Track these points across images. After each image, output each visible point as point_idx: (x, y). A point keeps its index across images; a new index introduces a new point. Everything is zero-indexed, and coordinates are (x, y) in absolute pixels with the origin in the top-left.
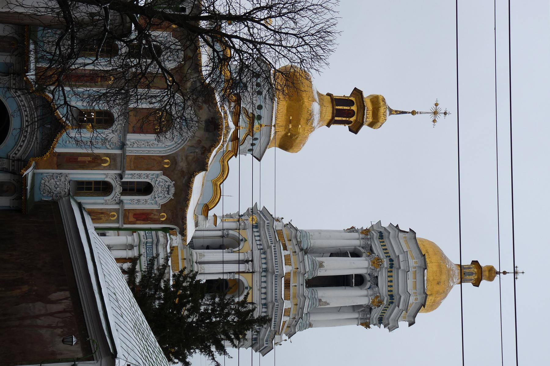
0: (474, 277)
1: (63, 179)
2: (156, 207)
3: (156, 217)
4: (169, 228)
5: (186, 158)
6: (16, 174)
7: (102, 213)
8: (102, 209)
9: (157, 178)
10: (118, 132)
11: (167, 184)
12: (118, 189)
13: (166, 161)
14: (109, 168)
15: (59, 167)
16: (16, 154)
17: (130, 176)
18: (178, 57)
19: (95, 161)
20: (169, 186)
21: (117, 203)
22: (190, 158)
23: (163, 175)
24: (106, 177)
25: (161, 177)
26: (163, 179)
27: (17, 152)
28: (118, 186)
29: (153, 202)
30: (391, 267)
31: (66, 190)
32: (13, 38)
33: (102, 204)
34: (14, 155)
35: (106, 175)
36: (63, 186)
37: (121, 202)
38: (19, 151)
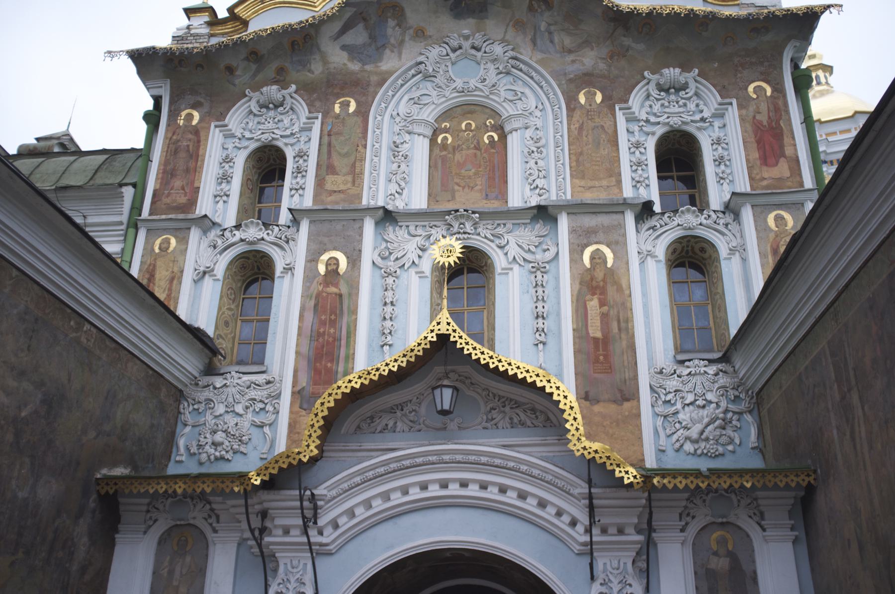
0: (821, 73)
1: (673, 384)
2: (733, 114)
3: (764, 107)
4: (792, 74)
5: (570, 51)
6: (651, 514)
7: (775, 251)
8: (763, 255)
9: (639, 121)
10: (500, 230)
11: (654, 93)
12: (689, 220)
13: (582, 99)
14: (619, 245)
15: (627, 394)
16: (573, 523)
17: (642, 191)
18: (282, 105)
19: (600, 287)
20: (660, 88)
21: (737, 216)
22: (567, 41)
23: (627, 101)
24: (654, 256)
25: (635, 108)
26: (642, 106)
27: (566, 519)
28: (677, 220)
29: (717, 123)
30: (825, 162)
31: (712, 370)
32: (161, 542)
33: (744, 260)
34: (580, 528)
35: (645, 256)
36: (698, 379)
37: (731, 209)
38: (559, 514)
